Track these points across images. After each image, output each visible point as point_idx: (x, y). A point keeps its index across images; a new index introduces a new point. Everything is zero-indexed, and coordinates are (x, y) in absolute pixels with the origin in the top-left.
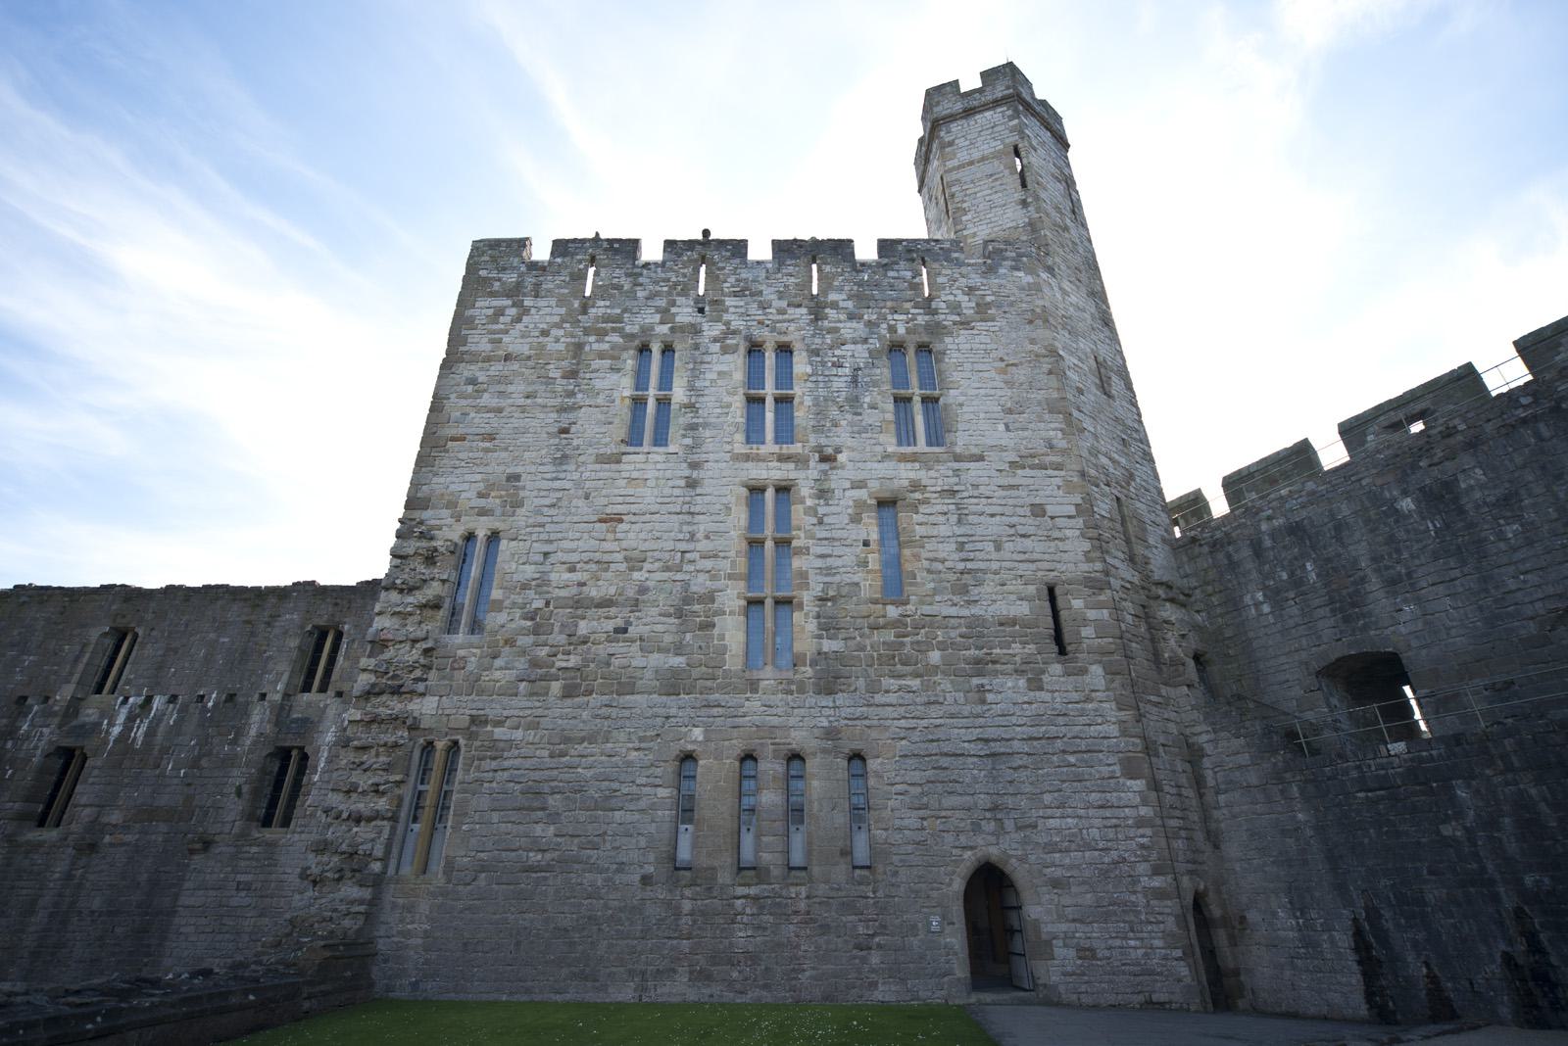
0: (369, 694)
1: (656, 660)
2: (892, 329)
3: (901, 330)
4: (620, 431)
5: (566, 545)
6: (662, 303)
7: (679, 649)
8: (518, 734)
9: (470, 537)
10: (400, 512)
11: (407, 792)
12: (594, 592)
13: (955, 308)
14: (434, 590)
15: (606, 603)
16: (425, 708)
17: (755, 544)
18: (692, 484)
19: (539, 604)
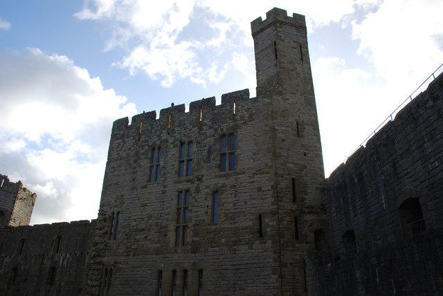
0: (95, 256)
1: (153, 245)
2: (222, 130)
3: (225, 130)
4: (146, 178)
5: (134, 214)
6: (158, 133)
7: (158, 242)
8: (124, 266)
9: (113, 213)
10: (98, 208)
11: (102, 280)
12: (140, 227)
13: (242, 118)
14: (106, 229)
15: (143, 230)
16: (105, 259)
17: (178, 209)
18: (164, 192)
19: (128, 231)
